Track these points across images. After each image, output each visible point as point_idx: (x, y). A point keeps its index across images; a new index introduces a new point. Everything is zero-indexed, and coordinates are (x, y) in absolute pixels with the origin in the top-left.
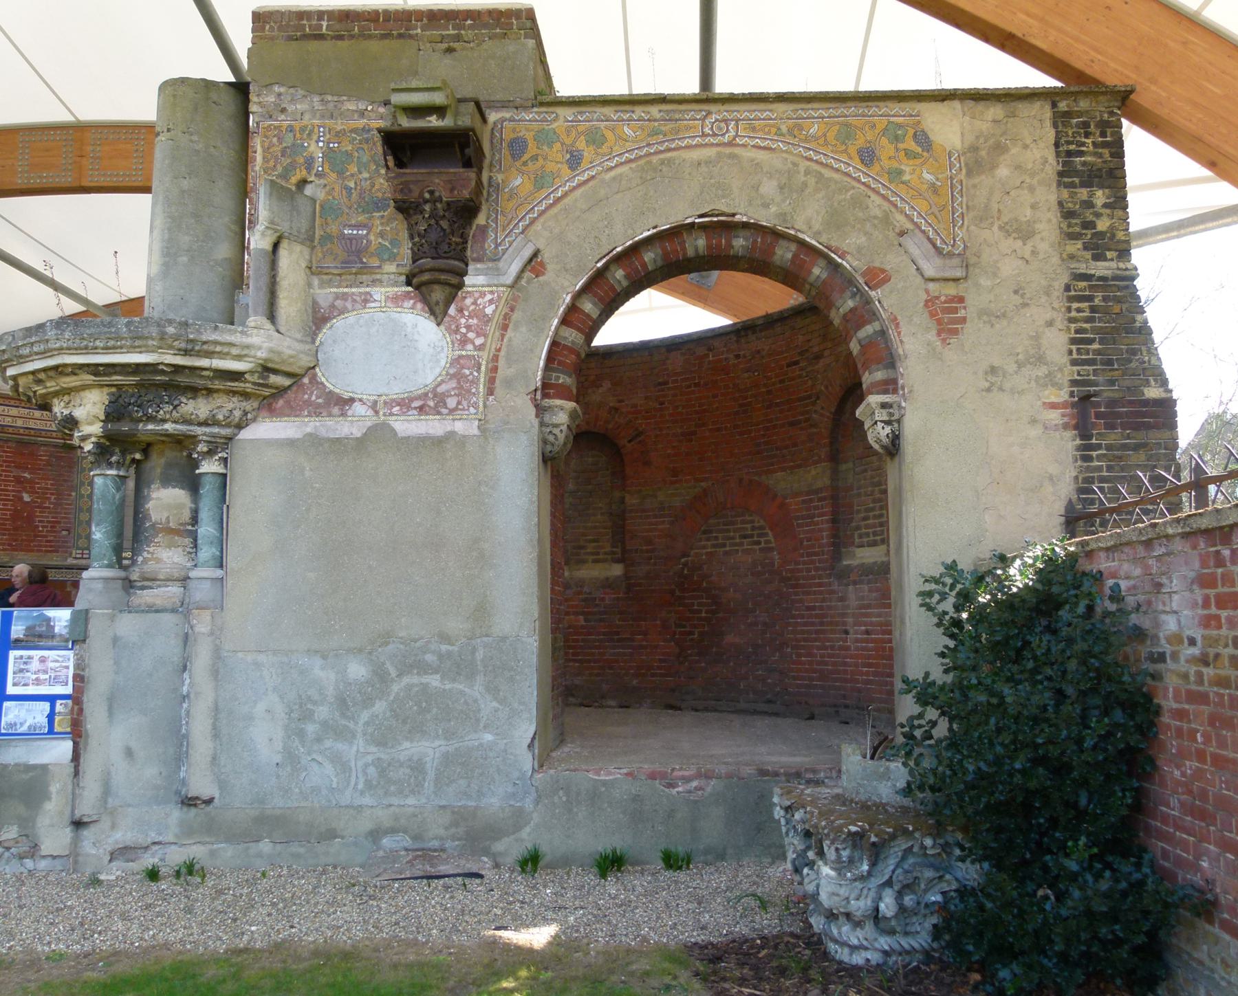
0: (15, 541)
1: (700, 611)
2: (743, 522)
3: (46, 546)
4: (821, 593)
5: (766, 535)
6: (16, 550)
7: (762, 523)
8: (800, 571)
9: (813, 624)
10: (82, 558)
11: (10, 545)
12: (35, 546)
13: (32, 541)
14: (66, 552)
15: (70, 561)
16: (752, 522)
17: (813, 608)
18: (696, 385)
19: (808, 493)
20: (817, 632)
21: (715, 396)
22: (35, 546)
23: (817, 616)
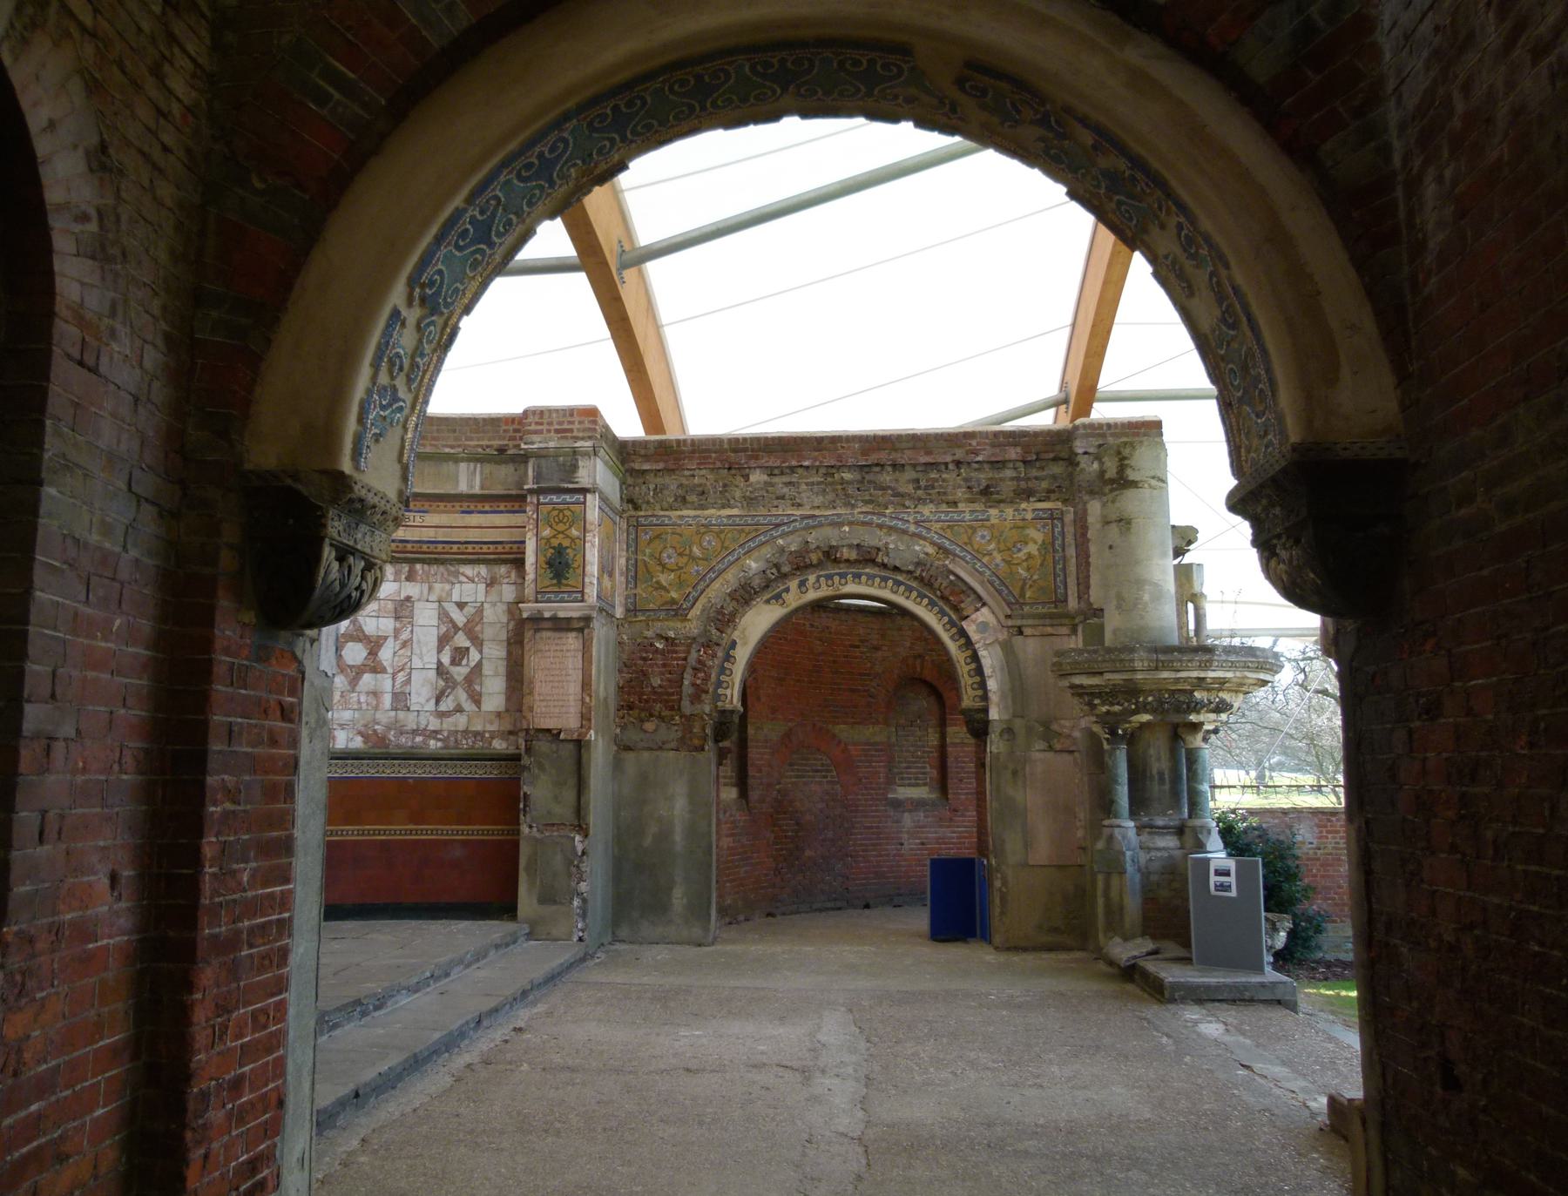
1: (787, 831)
2: (815, 759)
4: (878, 817)
5: (831, 771)
7: (829, 762)
8: (859, 800)
9: (871, 839)
16: (822, 759)
17: (871, 827)
18: (786, 639)
19: (866, 744)
20: (872, 845)
21: (797, 652)
23: (873, 833)
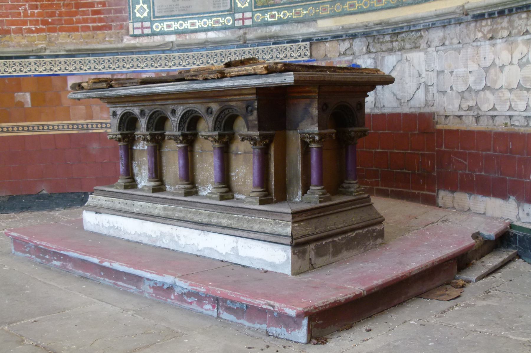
0: (52, 15)
3: (94, 21)
6: (54, 30)
10: (143, 35)
11: (45, 23)
12: (78, 22)
13: (76, 14)
14: (121, 27)
15: (128, 41)
22: (78, 22)
